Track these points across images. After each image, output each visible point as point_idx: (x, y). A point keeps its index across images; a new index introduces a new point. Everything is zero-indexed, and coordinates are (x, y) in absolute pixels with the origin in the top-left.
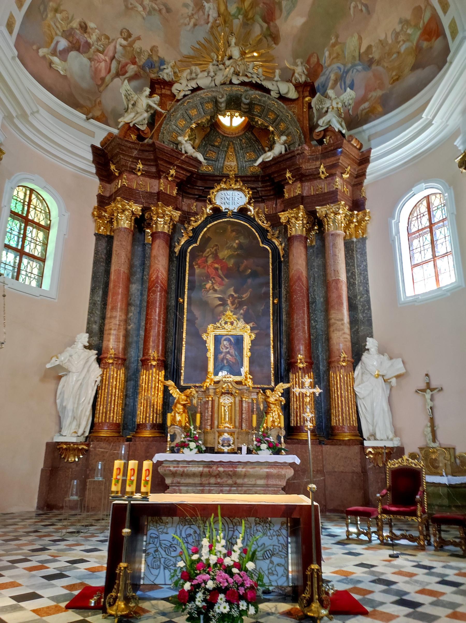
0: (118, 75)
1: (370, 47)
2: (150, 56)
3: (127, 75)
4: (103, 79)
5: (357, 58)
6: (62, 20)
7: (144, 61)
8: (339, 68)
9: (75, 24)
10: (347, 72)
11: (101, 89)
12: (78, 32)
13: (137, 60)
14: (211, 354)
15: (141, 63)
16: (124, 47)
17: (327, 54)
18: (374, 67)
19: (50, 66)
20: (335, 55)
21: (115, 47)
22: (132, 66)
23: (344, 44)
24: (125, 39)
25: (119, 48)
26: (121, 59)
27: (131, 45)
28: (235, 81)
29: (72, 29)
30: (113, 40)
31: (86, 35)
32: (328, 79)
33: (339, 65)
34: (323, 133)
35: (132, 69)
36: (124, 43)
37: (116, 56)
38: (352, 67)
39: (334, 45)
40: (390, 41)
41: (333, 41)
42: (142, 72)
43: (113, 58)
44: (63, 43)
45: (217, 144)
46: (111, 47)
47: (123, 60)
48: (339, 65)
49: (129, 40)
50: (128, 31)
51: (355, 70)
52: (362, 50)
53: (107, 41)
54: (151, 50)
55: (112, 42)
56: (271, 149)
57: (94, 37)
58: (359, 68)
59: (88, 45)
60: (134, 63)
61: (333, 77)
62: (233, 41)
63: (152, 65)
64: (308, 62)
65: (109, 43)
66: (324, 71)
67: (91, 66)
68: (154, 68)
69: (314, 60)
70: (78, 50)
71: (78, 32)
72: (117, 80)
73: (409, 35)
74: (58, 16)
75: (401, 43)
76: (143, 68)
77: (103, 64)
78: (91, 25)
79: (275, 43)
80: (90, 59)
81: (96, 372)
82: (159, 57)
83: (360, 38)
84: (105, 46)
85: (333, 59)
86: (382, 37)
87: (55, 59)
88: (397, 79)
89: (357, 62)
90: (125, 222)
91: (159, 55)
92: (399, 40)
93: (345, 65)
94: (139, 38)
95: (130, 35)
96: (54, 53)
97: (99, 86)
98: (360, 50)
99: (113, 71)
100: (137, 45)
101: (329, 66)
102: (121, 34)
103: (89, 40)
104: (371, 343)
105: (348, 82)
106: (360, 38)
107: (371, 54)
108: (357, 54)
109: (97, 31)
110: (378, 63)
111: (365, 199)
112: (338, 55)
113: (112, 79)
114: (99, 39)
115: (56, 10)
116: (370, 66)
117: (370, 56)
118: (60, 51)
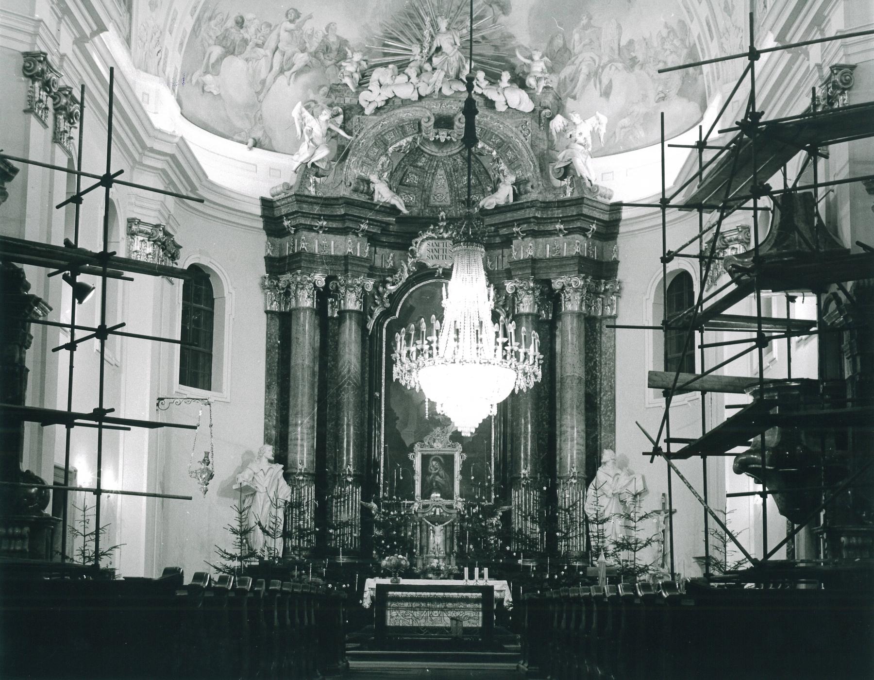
0: (282, 71)
1: (631, 42)
2: (325, 36)
3: (294, 69)
4: (263, 82)
5: (617, 52)
6: (216, 26)
7: (316, 45)
8: (594, 61)
9: (231, 23)
10: (603, 68)
11: (261, 97)
12: (233, 30)
13: (307, 45)
14: (418, 478)
15: (313, 49)
16: (290, 32)
17: (576, 37)
18: (637, 69)
19: (203, 91)
20: (587, 41)
21: (279, 35)
22: (302, 55)
23: (600, 28)
24: (291, 21)
25: (284, 35)
26: (286, 48)
27: (299, 28)
28: (446, 91)
29: (227, 30)
30: (277, 26)
31: (242, 31)
32: (578, 71)
33: (593, 55)
34: (563, 170)
35: (301, 59)
36: (291, 26)
37: (279, 46)
38: (610, 62)
39: (585, 28)
40: (655, 44)
41: (584, 21)
42: (314, 61)
43: (277, 48)
44: (217, 51)
45: (420, 164)
46: (274, 36)
47: (289, 52)
48: (593, 55)
49: (298, 21)
50: (296, 10)
51: (613, 68)
52: (623, 43)
53: (268, 29)
54: (327, 29)
55: (274, 29)
56: (495, 190)
57: (252, 30)
58: (620, 65)
59: (245, 42)
60: (303, 51)
61: (585, 70)
62: (443, 24)
63: (327, 49)
64: (551, 42)
65: (271, 31)
66: (573, 59)
67: (248, 69)
68: (330, 52)
69: (559, 42)
70: (233, 53)
71: (233, 30)
72: (282, 80)
73: (676, 47)
74: (213, 23)
75: (668, 52)
76: (315, 55)
77: (263, 62)
78: (248, 16)
79: (504, 13)
80: (247, 60)
81: (285, 492)
82: (338, 37)
83: (619, 27)
84: (265, 37)
85: (584, 45)
86: (647, 35)
87: (209, 78)
88: (663, 99)
89: (616, 57)
90: (305, 300)
91: (338, 33)
92: (665, 47)
93: (600, 57)
94: (310, 17)
95: (298, 16)
96: (206, 72)
97: (258, 93)
98: (619, 40)
99: (276, 68)
100: (307, 27)
101: (580, 53)
102: (287, 15)
103: (246, 36)
104: (607, 455)
105: (605, 81)
106: (619, 27)
107: (634, 51)
108: (616, 47)
109: (256, 21)
110: (642, 66)
111: (616, 262)
112: (591, 41)
113: (275, 79)
114: (258, 30)
115: (210, 19)
116: (632, 67)
117: (633, 55)
118: (213, 64)
